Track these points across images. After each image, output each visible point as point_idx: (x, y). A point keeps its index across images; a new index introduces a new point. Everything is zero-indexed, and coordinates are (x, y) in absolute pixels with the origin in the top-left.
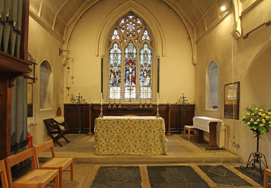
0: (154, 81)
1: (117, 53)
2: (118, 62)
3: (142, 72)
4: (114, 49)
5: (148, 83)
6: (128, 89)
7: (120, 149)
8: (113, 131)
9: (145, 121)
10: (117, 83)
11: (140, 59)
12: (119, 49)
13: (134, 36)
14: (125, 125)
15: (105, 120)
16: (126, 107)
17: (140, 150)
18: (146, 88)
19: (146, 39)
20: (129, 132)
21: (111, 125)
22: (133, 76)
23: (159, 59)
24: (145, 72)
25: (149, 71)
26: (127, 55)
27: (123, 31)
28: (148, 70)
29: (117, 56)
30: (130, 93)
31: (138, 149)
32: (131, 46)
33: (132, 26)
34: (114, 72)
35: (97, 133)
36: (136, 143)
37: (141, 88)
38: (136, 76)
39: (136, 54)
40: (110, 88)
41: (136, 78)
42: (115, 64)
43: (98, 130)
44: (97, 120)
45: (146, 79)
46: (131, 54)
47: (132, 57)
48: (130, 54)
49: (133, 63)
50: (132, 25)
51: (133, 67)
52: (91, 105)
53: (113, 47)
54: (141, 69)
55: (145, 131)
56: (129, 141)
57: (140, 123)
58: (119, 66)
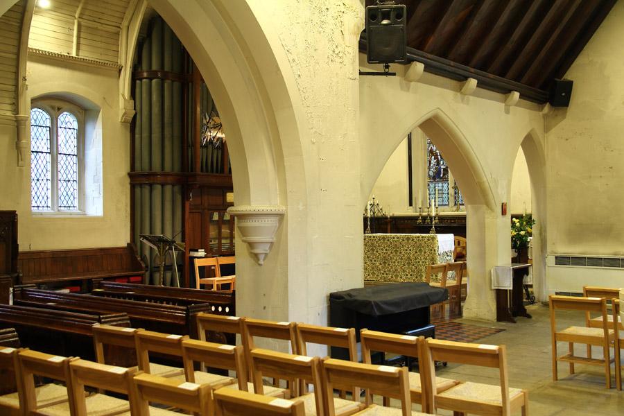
7: (387, 274)
10: (442, 175)
17: (409, 276)
20: (396, 251)
52: (391, 218)
56: (396, 264)
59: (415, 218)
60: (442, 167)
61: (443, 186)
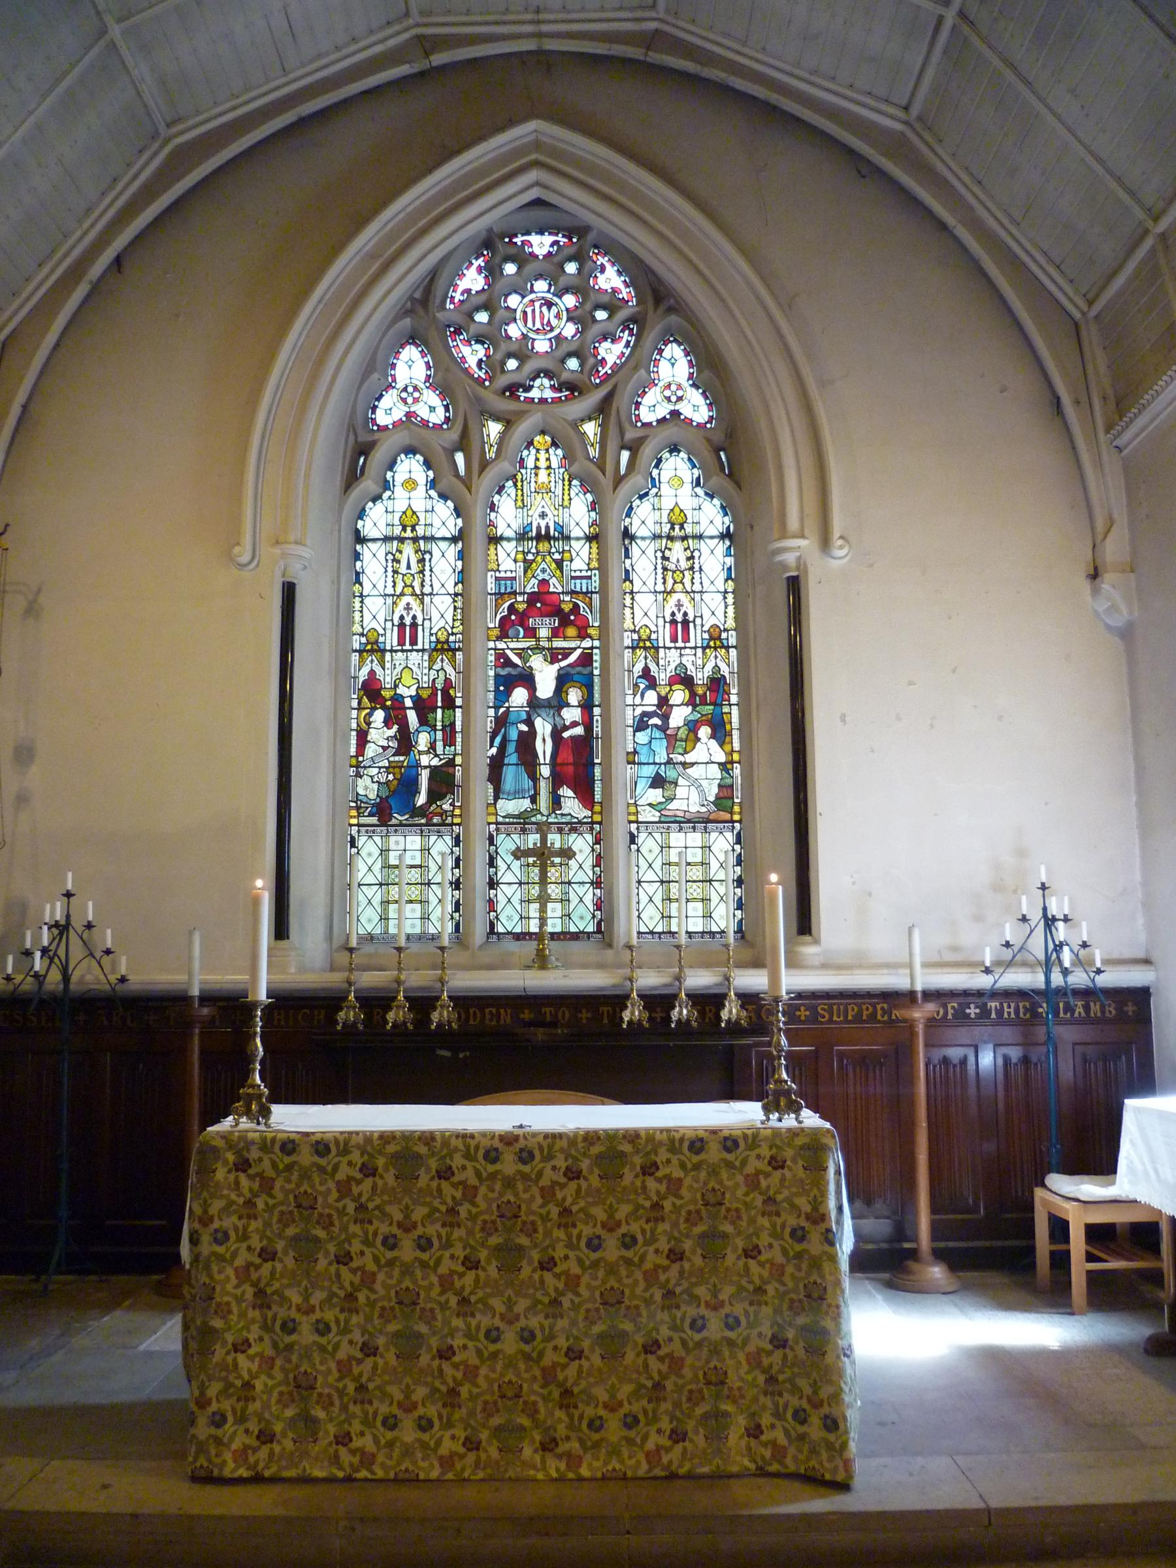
0: (763, 773)
1: (420, 531)
2: (436, 616)
3: (651, 697)
4: (400, 505)
5: (712, 791)
6: (518, 854)
8: (356, 1247)
9: (662, 1155)
10: (421, 799)
11: (627, 578)
12: (444, 497)
13: (573, 388)
14: (470, 1193)
15: (289, 1145)
16: (506, 1017)
17: (614, 1430)
18: (695, 839)
19: (675, 414)
20: (509, 1256)
21: (344, 1188)
22: (566, 728)
23: (795, 586)
24: (679, 695)
25: (717, 683)
26: (510, 546)
27: (472, 355)
28: (701, 677)
29: (421, 561)
30: (543, 881)
31: (596, 1425)
32: (543, 474)
33: (550, 315)
34: (398, 700)
35: (207, 1267)
36: (571, 1371)
37: (642, 837)
38: (597, 729)
39: (590, 539)
40: (362, 841)
41: (598, 746)
42: (402, 626)
43: (221, 1237)
44: (220, 1143)
45: (689, 758)
46: (543, 537)
47: (559, 564)
48: (539, 538)
49: (565, 621)
50: (549, 305)
51: (566, 653)
53: (386, 486)
54: (639, 667)
55: (664, 1245)
57: (611, 1176)
58: (442, 648)
59: (331, 1001)
60: (425, 760)
61: (425, 850)
